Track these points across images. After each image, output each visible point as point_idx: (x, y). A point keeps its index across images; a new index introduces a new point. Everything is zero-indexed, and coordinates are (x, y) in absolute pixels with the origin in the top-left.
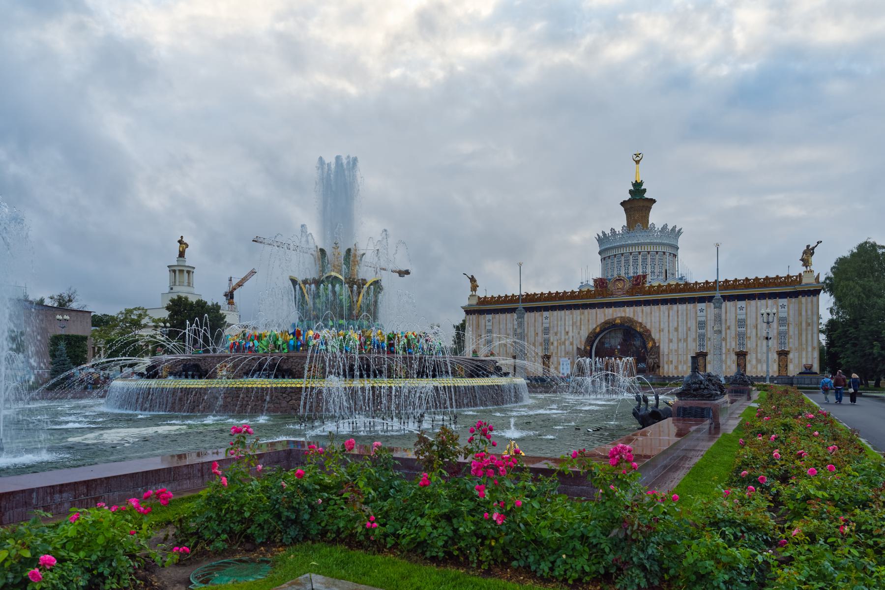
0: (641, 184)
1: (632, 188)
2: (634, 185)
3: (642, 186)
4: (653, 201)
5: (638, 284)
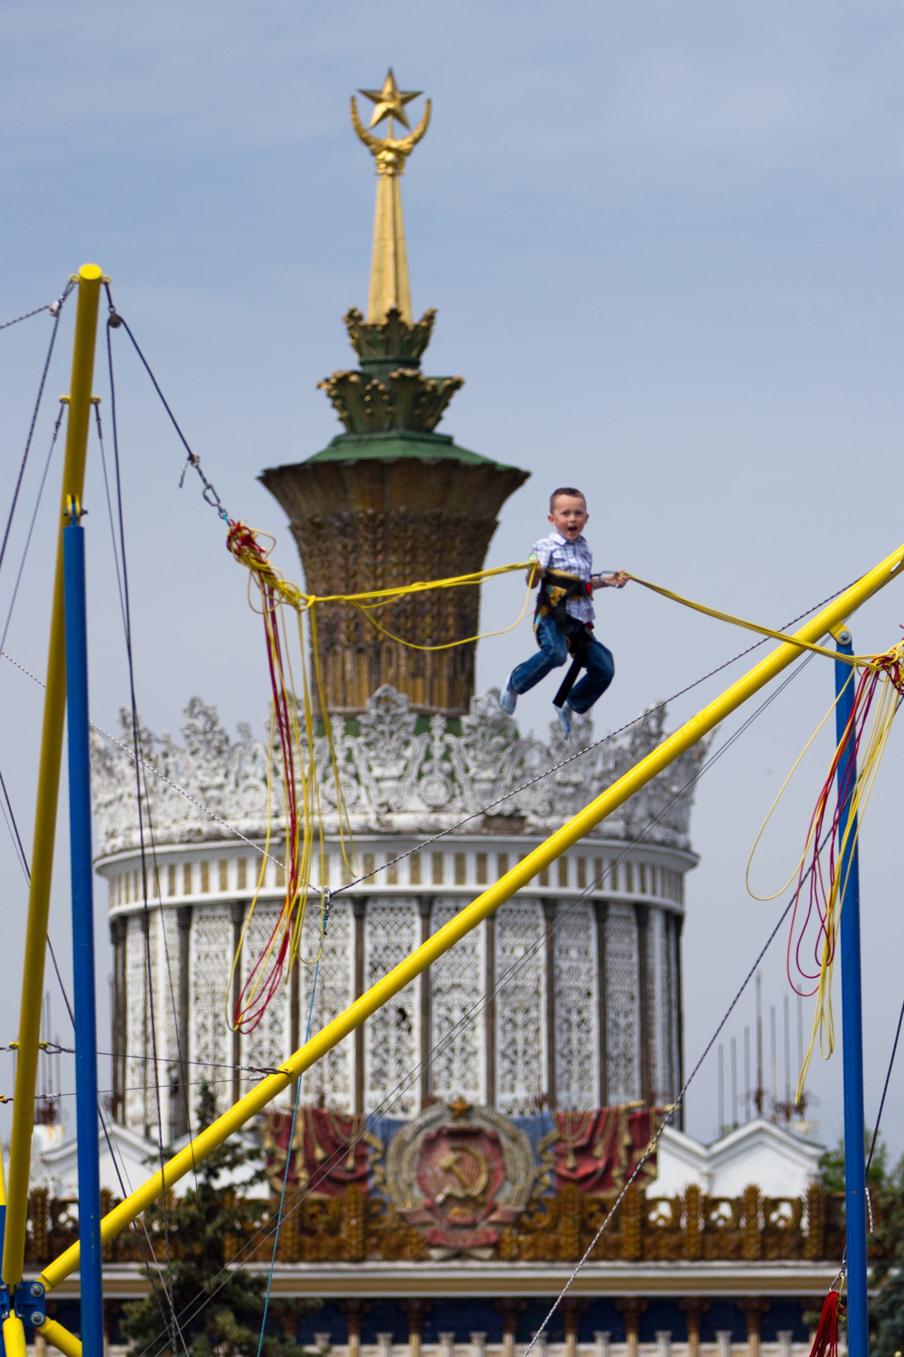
5: (604, 1180)
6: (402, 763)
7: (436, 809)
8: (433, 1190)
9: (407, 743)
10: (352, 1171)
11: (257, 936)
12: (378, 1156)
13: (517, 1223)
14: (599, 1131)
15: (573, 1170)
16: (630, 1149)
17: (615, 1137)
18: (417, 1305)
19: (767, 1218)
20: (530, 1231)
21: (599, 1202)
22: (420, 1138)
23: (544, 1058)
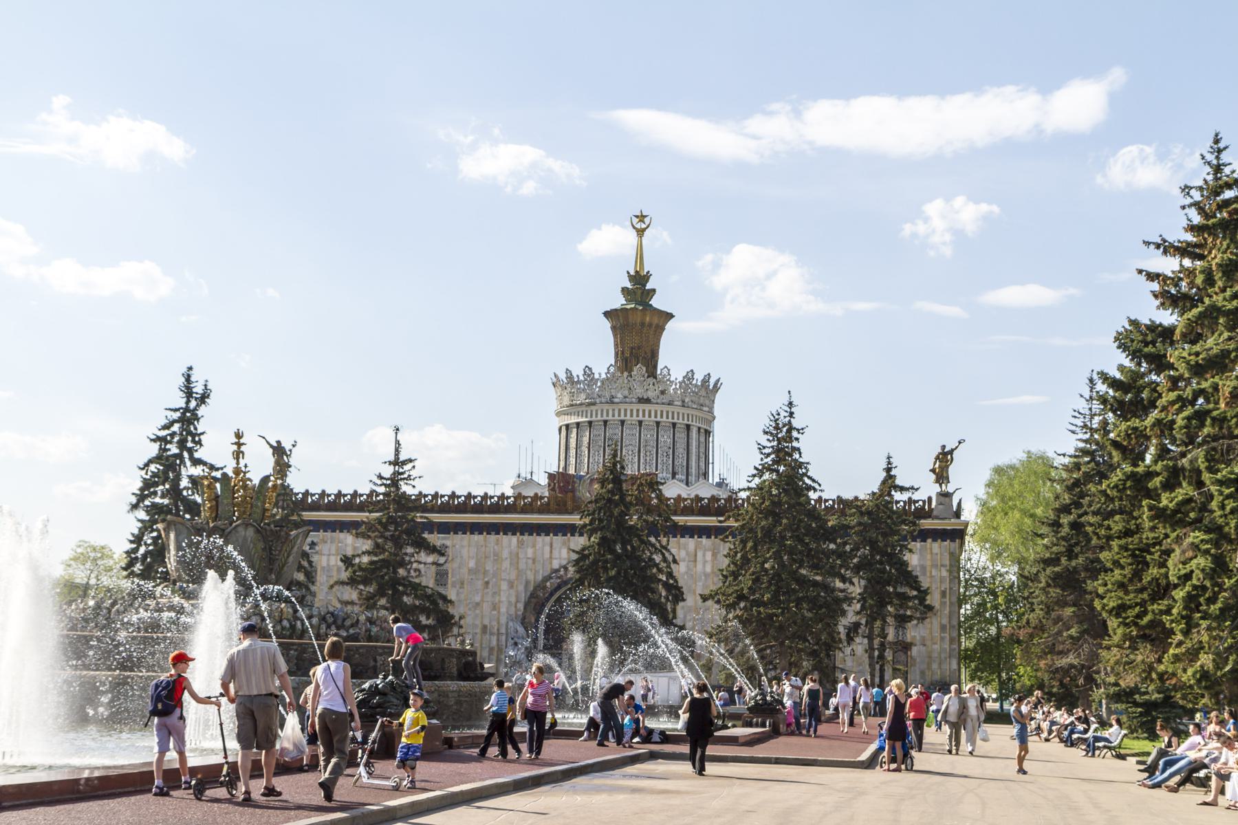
0: (647, 277)
1: (629, 285)
2: (632, 278)
3: (647, 281)
4: (670, 316)
7: (625, 397)
23: (654, 465)
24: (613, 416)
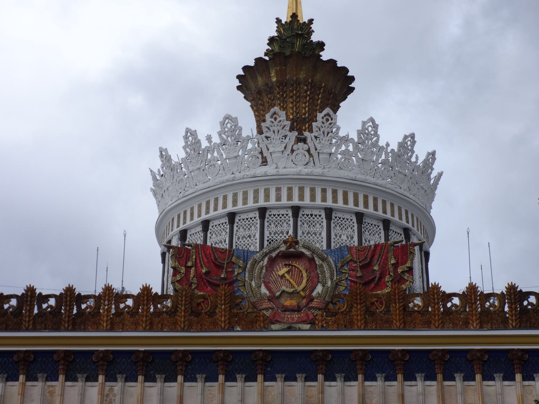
5: (380, 283)
6: (284, 145)
8: (274, 290)
9: (285, 136)
10: (224, 279)
11: (214, 236)
12: (240, 271)
13: (325, 309)
14: (376, 257)
15: (360, 277)
16: (395, 266)
17: (387, 259)
18: (261, 355)
19: (482, 306)
20: (335, 314)
21: (377, 296)
22: (266, 260)
24: (278, 199)
